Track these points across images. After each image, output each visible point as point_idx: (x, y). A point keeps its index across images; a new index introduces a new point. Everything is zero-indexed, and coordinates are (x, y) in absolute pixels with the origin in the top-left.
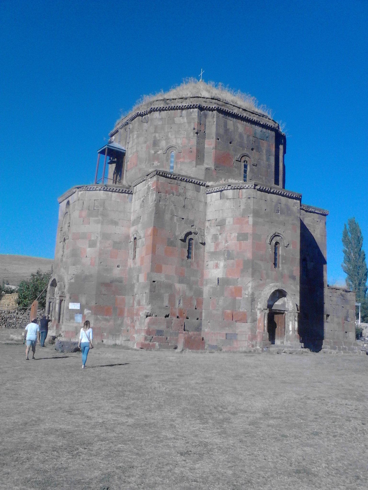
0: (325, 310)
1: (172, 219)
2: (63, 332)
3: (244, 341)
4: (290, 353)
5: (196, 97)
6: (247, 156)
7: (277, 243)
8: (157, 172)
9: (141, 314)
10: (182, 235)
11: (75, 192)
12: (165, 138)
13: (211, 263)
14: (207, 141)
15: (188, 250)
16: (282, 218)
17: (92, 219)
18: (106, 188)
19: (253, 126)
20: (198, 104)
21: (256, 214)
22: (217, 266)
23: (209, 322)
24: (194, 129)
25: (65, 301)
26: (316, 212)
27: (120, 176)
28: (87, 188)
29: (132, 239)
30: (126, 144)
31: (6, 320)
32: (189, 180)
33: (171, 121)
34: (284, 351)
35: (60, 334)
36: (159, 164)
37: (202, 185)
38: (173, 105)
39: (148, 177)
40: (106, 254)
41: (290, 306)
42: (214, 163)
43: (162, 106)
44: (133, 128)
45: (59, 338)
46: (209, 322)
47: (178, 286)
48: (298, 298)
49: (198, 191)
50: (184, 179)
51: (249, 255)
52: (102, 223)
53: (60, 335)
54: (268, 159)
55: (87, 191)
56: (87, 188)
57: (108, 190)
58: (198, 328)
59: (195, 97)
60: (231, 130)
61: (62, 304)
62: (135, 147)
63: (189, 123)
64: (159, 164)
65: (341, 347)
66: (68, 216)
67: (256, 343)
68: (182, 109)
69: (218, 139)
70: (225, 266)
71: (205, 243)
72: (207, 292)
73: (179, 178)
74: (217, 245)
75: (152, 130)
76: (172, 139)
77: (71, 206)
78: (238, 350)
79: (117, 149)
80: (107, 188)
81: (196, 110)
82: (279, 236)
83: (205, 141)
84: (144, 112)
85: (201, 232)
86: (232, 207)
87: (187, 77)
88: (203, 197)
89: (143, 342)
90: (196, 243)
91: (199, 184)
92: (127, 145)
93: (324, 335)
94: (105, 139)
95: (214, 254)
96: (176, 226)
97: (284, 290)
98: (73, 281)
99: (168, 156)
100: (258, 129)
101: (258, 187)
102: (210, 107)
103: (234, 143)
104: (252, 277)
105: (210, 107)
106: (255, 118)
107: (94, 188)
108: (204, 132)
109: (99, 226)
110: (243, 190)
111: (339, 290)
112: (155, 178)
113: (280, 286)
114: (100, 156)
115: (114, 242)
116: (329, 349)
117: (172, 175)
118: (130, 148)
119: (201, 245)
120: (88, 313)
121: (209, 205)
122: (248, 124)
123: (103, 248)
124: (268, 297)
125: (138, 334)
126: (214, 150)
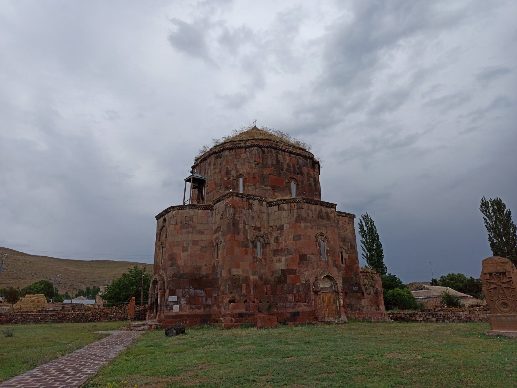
9: (225, 301)
11: (170, 211)
16: (324, 222)
17: (184, 230)
22: (280, 261)
29: (215, 244)
30: (205, 174)
44: (210, 162)
49: (262, 205)
52: (192, 234)
55: (180, 210)
60: (281, 161)
62: (213, 176)
70: (286, 260)
77: (167, 222)
82: (323, 235)
86: (288, 216)
92: (206, 175)
100: (301, 160)
103: (285, 169)
109: (190, 235)
115: (201, 247)
123: (193, 252)
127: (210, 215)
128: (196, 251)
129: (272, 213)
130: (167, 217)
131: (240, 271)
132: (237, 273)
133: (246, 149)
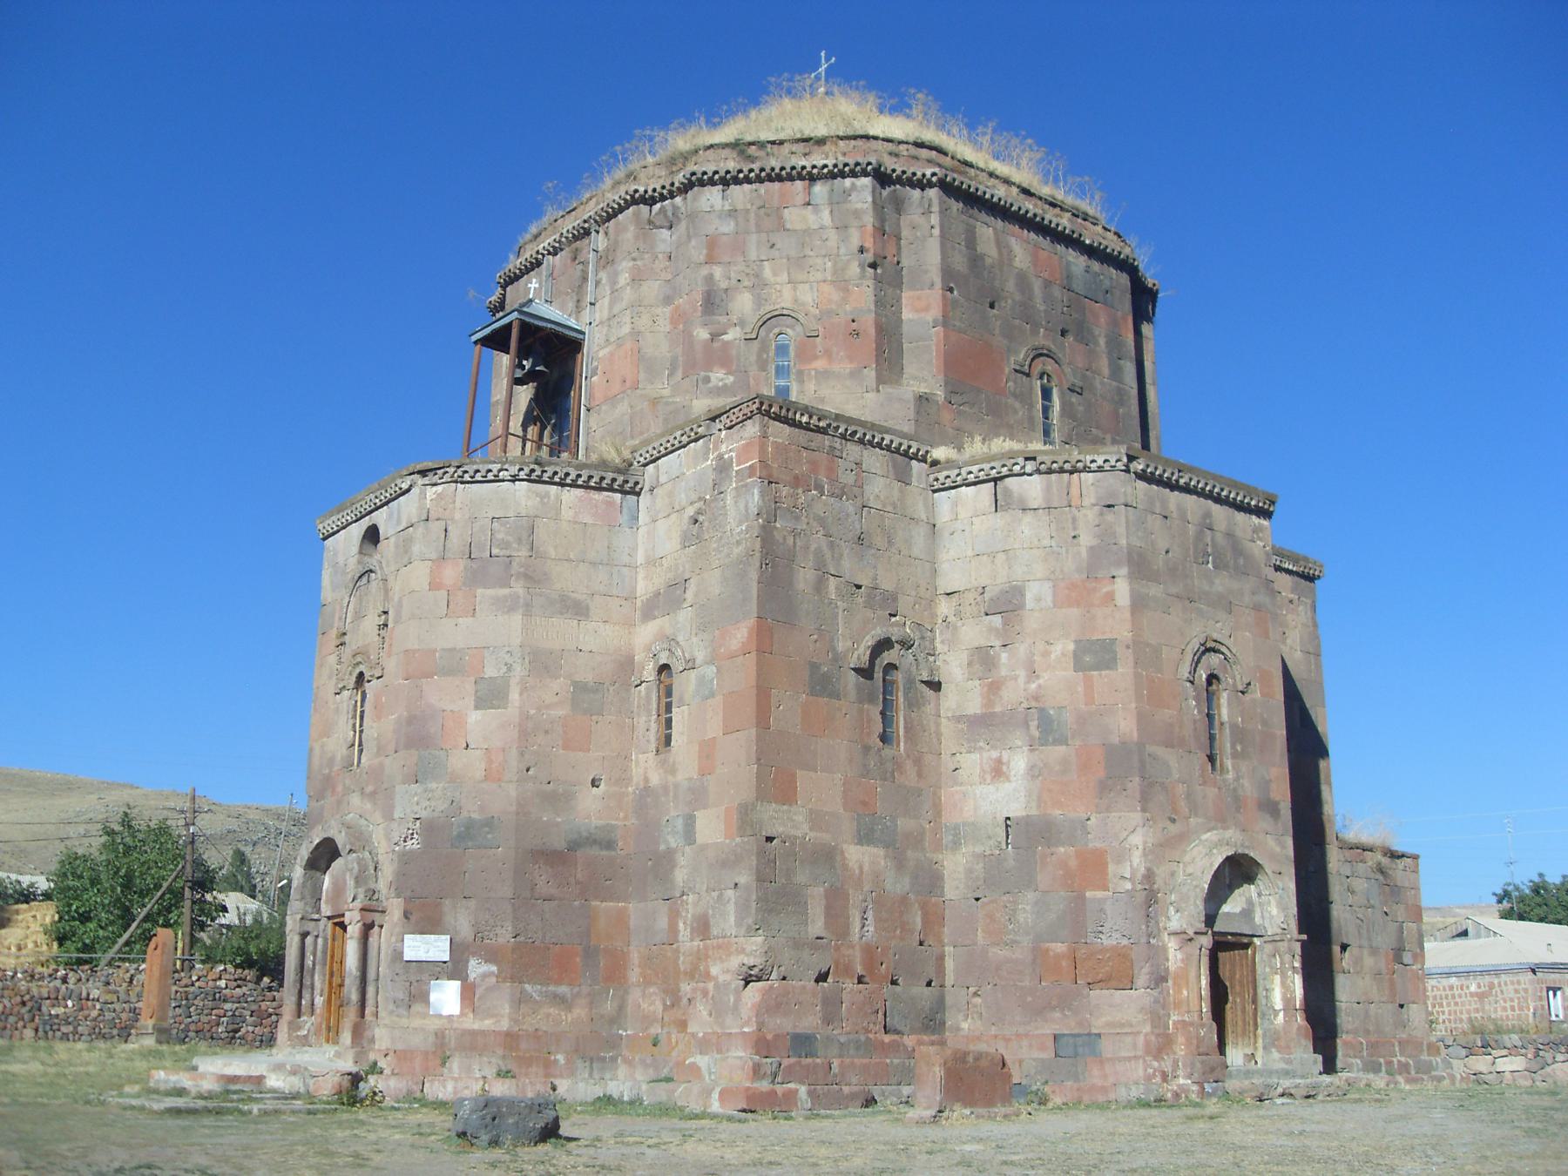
0: (1334, 925)
1: (820, 585)
2: (386, 1055)
3: (1129, 1059)
4: (1308, 1097)
5: (862, 137)
6: (1047, 356)
7: (1212, 678)
8: (762, 404)
9: (714, 971)
10: (861, 650)
11: (408, 491)
12: (746, 283)
13: (972, 762)
14: (906, 296)
15: (883, 713)
16: (1222, 583)
18: (538, 473)
19: (1060, 248)
20: (874, 161)
21: (1140, 566)
22: (998, 771)
23: (976, 994)
24: (862, 250)
25: (381, 927)
26: (1286, 566)
27: (559, 428)
28: (460, 472)
29: (649, 672)
30: (578, 308)
31: (36, 1005)
32: (874, 437)
33: (773, 220)
34: (1280, 1090)
35: (375, 1063)
36: (731, 379)
37: (915, 457)
38: (774, 163)
39: (718, 425)
40: (546, 732)
41: (1272, 917)
42: (941, 377)
43: (732, 165)
45: (372, 1080)
46: (976, 994)
47: (858, 856)
48: (1292, 886)
49: (903, 478)
50: (855, 433)
51: (1124, 725)
53: (374, 1069)
54: (1116, 373)
56: (460, 472)
57: (545, 477)
58: (933, 1022)
59: (855, 138)
60: (988, 261)
61: (371, 939)
62: (627, 319)
63: (842, 228)
64: (731, 379)
65: (1395, 1060)
66: (374, 584)
67: (1176, 1062)
68: (812, 179)
69: (951, 290)
70: (1033, 772)
71: (939, 684)
72: (963, 876)
73: (837, 428)
74: (994, 688)
75: (697, 251)
76: (778, 287)
77: (387, 547)
78: (1112, 1096)
79: (553, 326)
80: (543, 472)
81: (866, 181)
83: (899, 300)
84: (659, 190)
85: (923, 638)
86: (1046, 542)
87: (786, 75)
88: (920, 506)
89: (748, 1084)
90: (910, 682)
91: (906, 454)
93: (1339, 1021)
94: (472, 293)
95: (984, 725)
96: (836, 616)
97: (1252, 855)
98: (414, 845)
99: (764, 348)
100: (1078, 262)
101: (1138, 466)
102: (914, 174)
103: (1006, 305)
104: (1144, 810)
105: (914, 174)
106: (1064, 222)
107: (490, 471)
108: (898, 263)
109: (517, 619)
110: (1082, 474)
111: (1371, 850)
112: (752, 429)
113: (1239, 843)
114: (480, 351)
115: (575, 684)
116: (1358, 1071)
117: (815, 418)
118: (601, 323)
119: (924, 688)
120: (485, 976)
121: (946, 534)
122: (1045, 243)
123: (532, 712)
124: (1206, 886)
125: (719, 1056)
126: (939, 329)
127: (624, 519)
128: (548, 707)
129: (958, 525)
130: (390, 516)
131: (800, 818)
132: (781, 829)
133: (810, 186)
